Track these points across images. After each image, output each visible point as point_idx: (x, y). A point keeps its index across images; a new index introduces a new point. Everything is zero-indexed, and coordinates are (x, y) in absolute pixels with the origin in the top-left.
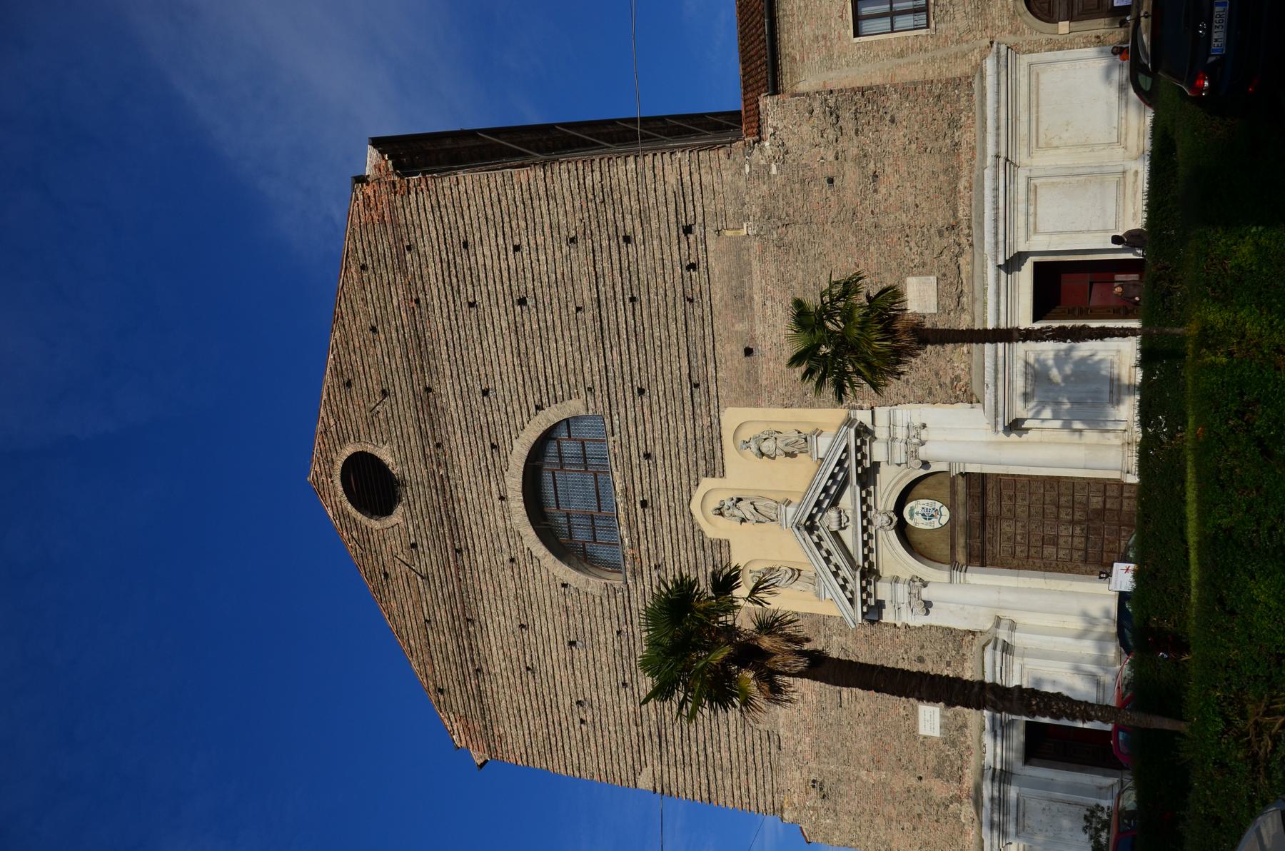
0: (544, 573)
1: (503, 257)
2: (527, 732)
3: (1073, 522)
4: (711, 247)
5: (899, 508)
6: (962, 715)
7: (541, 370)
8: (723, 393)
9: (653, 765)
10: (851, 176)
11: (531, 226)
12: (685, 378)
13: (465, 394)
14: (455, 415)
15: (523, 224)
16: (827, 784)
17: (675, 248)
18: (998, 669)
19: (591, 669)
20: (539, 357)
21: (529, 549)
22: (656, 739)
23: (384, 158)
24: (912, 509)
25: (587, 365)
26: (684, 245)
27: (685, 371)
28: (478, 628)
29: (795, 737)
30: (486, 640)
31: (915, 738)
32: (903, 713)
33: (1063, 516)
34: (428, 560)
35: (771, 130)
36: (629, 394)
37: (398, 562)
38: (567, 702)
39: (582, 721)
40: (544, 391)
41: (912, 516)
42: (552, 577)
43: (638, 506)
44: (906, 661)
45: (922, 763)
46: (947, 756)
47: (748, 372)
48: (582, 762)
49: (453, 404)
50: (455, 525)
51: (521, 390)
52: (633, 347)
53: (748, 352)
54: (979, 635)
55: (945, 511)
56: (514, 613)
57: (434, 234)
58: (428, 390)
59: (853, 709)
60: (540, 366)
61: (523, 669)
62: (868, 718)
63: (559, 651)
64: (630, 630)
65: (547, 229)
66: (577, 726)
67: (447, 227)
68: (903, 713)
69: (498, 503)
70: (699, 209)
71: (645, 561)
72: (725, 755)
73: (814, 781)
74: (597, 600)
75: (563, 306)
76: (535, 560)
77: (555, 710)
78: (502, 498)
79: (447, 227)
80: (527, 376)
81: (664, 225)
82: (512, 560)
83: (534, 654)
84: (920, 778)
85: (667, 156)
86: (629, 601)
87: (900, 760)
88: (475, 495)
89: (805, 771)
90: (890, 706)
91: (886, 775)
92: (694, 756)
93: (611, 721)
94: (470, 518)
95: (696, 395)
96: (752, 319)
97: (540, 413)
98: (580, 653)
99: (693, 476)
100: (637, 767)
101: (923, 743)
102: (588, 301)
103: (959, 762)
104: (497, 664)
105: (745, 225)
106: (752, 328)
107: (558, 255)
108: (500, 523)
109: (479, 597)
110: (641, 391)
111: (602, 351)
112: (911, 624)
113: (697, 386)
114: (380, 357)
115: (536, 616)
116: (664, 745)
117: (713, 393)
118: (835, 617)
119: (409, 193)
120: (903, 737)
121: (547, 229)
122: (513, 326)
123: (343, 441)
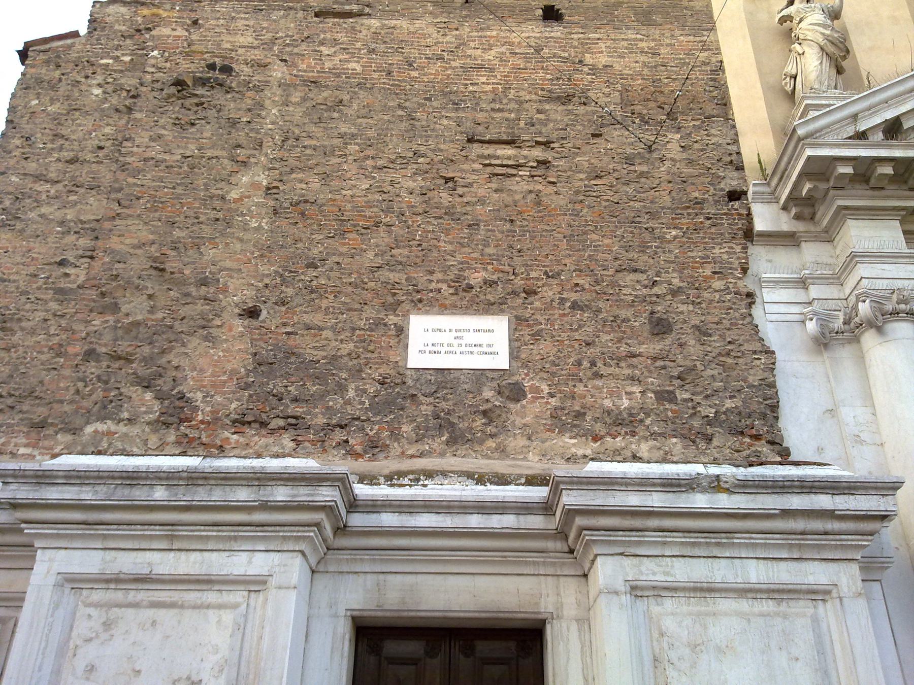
6: (489, 430)
16: (219, 97)
18: (824, 501)
29: (358, 45)
31: (393, 307)
32: (476, 278)
44: (645, 291)
45: (307, 318)
46: (341, 388)
59: (465, 167)
62: (445, 197)
68: (476, 278)
73: (227, 70)
84: (252, 313)
87: (312, 265)
89: (257, 54)
90: (490, 250)
91: (259, 228)
101: (379, 323)
103: (321, 420)
118: (736, 141)
120: (393, 277)
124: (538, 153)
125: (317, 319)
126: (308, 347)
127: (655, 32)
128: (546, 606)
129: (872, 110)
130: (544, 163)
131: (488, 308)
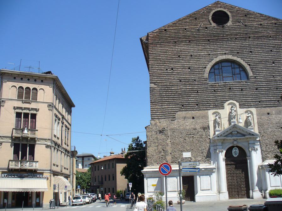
0: (208, 63)
5: (237, 147)
12: (261, 100)
14: (244, 44)
20: (261, 66)
22: (166, 89)
24: (237, 149)
27: (263, 100)
41: (235, 149)
43: (229, 88)
47: (264, 114)
49: (247, 44)
52: (267, 88)
53: (268, 114)
55: (236, 156)
58: (249, 37)
60: (260, 66)
61: (179, 55)
63: (187, 65)
64: (197, 83)
66: (165, 68)
69: (224, 52)
72: (166, 107)
73: (164, 128)
74: (203, 76)
76: (211, 61)
78: (225, 53)
82: (209, 54)
86: (204, 84)
89: (166, 126)
93: (169, 77)
96: (276, 114)
97: (248, 65)
99: (239, 101)
102: (276, 78)
104: (178, 48)
106: (274, 115)
108: (219, 53)
109: (197, 45)
111: (265, 81)
112: (210, 150)
116: (165, 91)
123: (231, 12)
124: (193, 136)
126: (175, 156)
127: (203, 120)
128: (194, 174)
130: (193, 137)
131: (190, 151)
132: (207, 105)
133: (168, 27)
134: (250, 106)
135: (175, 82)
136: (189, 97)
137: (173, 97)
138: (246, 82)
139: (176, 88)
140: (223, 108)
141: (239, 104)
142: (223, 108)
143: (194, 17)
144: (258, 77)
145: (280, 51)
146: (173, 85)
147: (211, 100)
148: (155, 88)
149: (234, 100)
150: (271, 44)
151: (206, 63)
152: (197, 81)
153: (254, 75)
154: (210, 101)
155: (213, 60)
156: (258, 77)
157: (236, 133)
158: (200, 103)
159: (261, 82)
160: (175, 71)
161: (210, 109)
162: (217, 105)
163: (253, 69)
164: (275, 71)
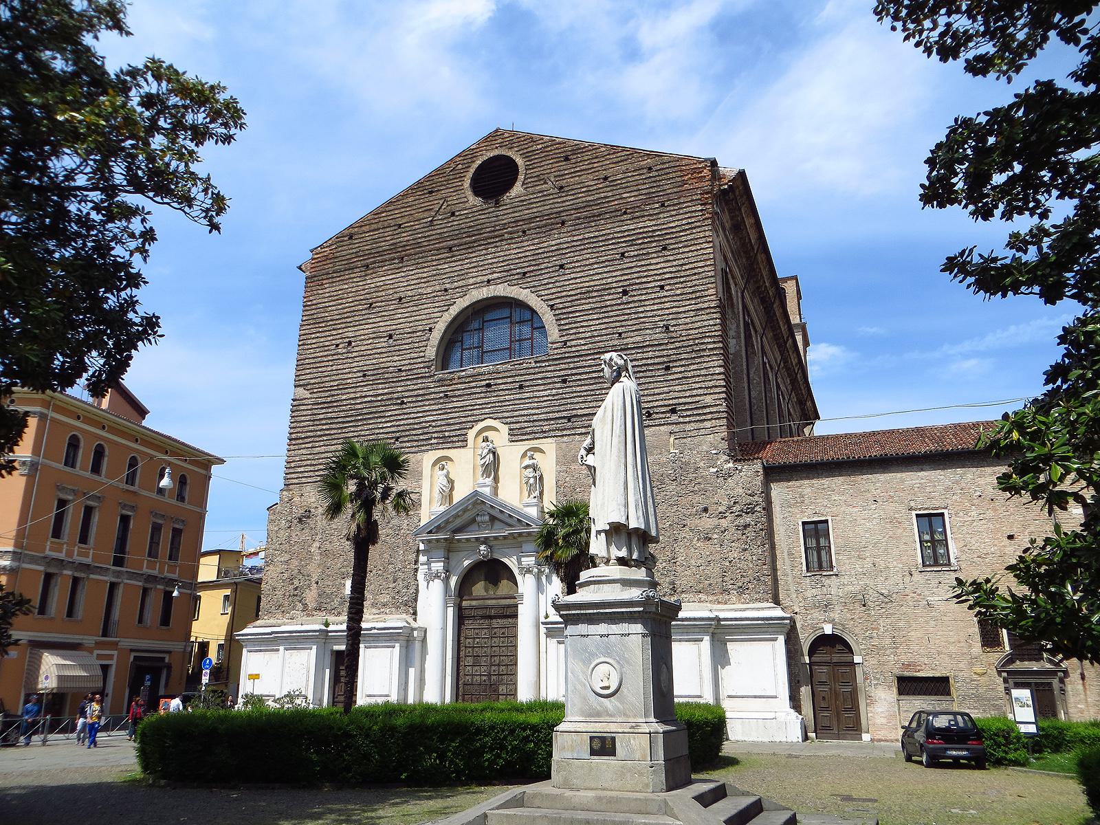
1: (656, 278)
2: (327, 304)
3: (489, 675)
4: (662, 428)
7: (578, 308)
8: (565, 439)
9: (311, 398)
10: (707, 522)
11: (678, 298)
12: (574, 412)
13: (561, 252)
14: (545, 244)
15: (678, 292)
17: (661, 403)
19: (374, 351)
21: (455, 302)
22: (329, 400)
23: (729, 181)
25: (582, 342)
26: (663, 409)
27: (580, 412)
28: (397, 266)
30: (389, 272)
33: (493, 668)
34: (444, 226)
35: (740, 468)
36: (562, 373)
37: (441, 202)
38: (350, 334)
39: (337, 345)
40: (564, 311)
42: (436, 320)
48: (309, 346)
49: (554, 243)
50: (469, 247)
51: (564, 294)
54: (414, 616)
56: (409, 293)
57: (672, 225)
58: (563, 223)
63: (384, 326)
65: (675, 310)
67: (677, 235)
69: (485, 278)
70: (687, 419)
71: (450, 388)
73: (310, 511)
74: (422, 354)
75: (623, 323)
76: (447, 307)
77: (343, 325)
78: (489, 281)
79: (677, 235)
80: (574, 298)
81: (677, 395)
82: (446, 290)
83: (382, 309)
85: (724, 395)
86: (422, 377)
88: (490, 261)
92: (320, 427)
94: (475, 258)
95: (563, 421)
98: (383, 343)
100: (309, 387)
101: (341, 583)
102: (625, 341)
104: (373, 281)
105: (677, 451)
107: (657, 319)
108: (471, 281)
110: (564, 381)
113: (569, 421)
114: (586, 184)
115: (409, 309)
116: (326, 405)
117: (564, 433)
119: (701, 205)
121: (675, 310)
122: (607, 287)
123: (525, 156)
125: (329, 583)
129: (431, 525)
132: (421, 437)
133: (361, 226)
134: (544, 434)
135: (355, 377)
136: (380, 417)
137: (343, 422)
138: (536, 362)
139: (352, 396)
140: (463, 443)
141: (510, 430)
142: (463, 443)
143: (427, 187)
144: (573, 343)
145: (648, 253)
146: (347, 388)
147: (434, 424)
148: (305, 399)
149: (495, 419)
150: (626, 234)
151: (435, 315)
152: (406, 370)
153: (563, 336)
154: (430, 426)
155: (454, 306)
156: (573, 343)
157: (487, 518)
158: (403, 434)
159: (582, 356)
160: (357, 349)
161: (427, 451)
162: (450, 437)
163: (561, 319)
164: (626, 317)
